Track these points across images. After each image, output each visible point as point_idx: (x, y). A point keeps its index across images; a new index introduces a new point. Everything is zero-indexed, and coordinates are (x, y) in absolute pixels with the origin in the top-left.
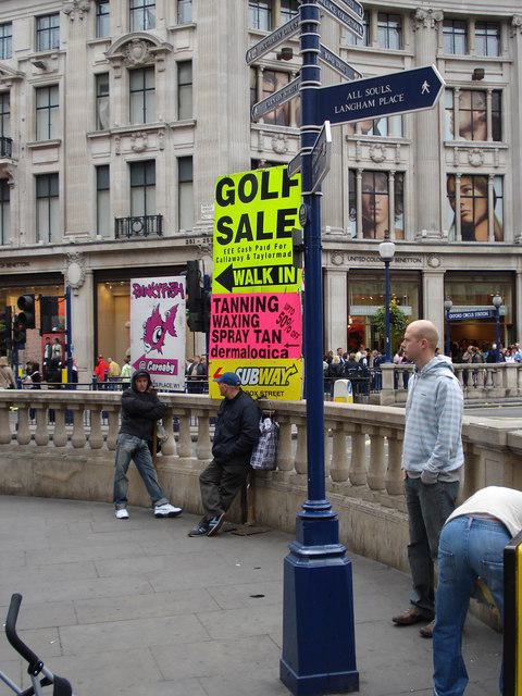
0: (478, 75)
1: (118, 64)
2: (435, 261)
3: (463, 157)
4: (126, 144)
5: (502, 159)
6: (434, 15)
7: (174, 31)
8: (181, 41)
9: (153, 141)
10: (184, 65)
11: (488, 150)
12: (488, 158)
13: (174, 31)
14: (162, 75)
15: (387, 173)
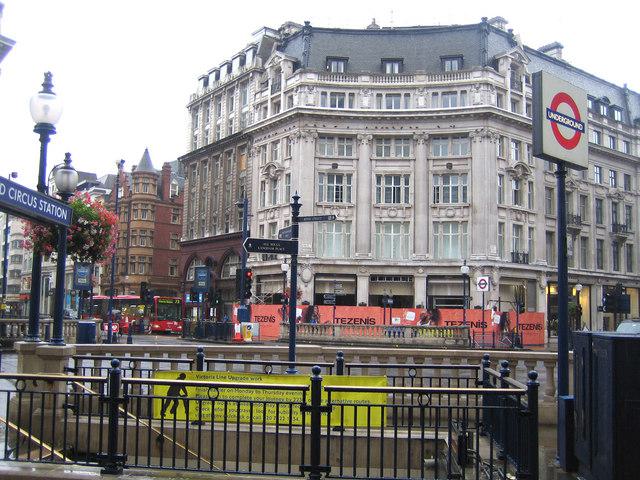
0: (450, 166)
4: (270, 215)
10: (288, 175)
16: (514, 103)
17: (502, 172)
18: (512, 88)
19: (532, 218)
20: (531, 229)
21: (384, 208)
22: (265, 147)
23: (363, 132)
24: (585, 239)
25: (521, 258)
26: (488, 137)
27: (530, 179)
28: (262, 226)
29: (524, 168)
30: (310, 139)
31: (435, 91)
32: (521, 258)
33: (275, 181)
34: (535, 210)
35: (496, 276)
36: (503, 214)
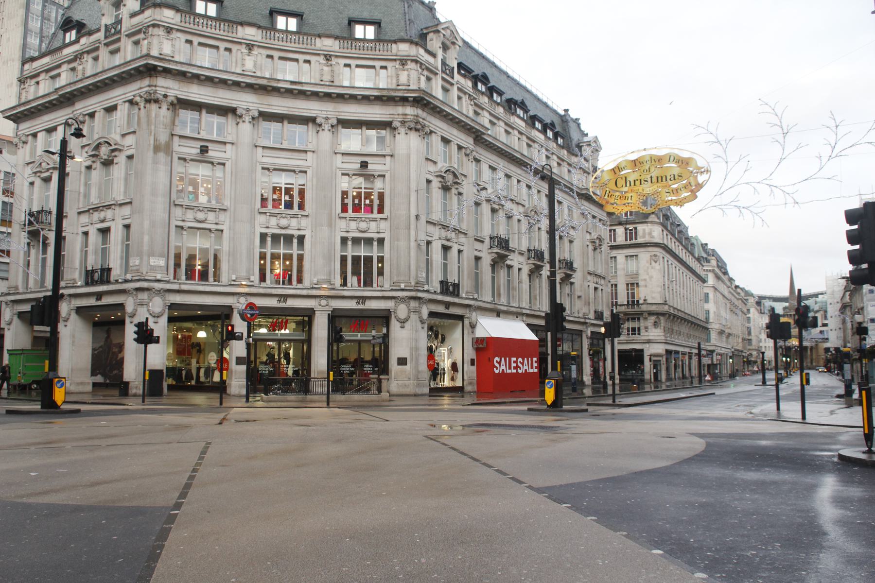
1: (94, 159)
2: (324, 302)
3: (353, 225)
4: (96, 216)
5: (383, 225)
6: (330, 121)
7: (123, 135)
8: (130, 140)
9: (109, 214)
11: (375, 220)
12: (373, 225)
13: (123, 135)
14: (117, 165)
15: (292, 236)
16: (445, 90)
17: (430, 177)
18: (443, 71)
19: (462, 239)
20: (460, 251)
21: (273, 215)
22: (92, 115)
23: (244, 105)
24: (510, 267)
25: (451, 289)
26: (417, 130)
27: (461, 190)
28: (86, 234)
29: (455, 176)
30: (165, 107)
31: (348, 61)
32: (451, 289)
33: (108, 163)
34: (464, 227)
35: (425, 312)
36: (431, 228)
